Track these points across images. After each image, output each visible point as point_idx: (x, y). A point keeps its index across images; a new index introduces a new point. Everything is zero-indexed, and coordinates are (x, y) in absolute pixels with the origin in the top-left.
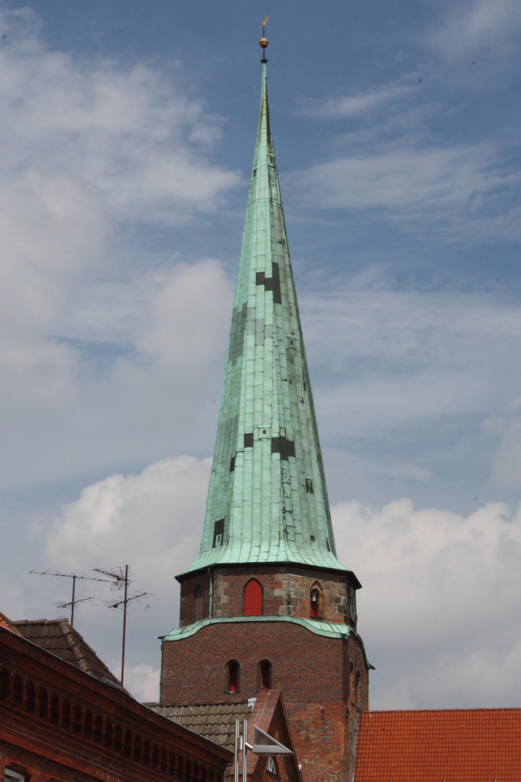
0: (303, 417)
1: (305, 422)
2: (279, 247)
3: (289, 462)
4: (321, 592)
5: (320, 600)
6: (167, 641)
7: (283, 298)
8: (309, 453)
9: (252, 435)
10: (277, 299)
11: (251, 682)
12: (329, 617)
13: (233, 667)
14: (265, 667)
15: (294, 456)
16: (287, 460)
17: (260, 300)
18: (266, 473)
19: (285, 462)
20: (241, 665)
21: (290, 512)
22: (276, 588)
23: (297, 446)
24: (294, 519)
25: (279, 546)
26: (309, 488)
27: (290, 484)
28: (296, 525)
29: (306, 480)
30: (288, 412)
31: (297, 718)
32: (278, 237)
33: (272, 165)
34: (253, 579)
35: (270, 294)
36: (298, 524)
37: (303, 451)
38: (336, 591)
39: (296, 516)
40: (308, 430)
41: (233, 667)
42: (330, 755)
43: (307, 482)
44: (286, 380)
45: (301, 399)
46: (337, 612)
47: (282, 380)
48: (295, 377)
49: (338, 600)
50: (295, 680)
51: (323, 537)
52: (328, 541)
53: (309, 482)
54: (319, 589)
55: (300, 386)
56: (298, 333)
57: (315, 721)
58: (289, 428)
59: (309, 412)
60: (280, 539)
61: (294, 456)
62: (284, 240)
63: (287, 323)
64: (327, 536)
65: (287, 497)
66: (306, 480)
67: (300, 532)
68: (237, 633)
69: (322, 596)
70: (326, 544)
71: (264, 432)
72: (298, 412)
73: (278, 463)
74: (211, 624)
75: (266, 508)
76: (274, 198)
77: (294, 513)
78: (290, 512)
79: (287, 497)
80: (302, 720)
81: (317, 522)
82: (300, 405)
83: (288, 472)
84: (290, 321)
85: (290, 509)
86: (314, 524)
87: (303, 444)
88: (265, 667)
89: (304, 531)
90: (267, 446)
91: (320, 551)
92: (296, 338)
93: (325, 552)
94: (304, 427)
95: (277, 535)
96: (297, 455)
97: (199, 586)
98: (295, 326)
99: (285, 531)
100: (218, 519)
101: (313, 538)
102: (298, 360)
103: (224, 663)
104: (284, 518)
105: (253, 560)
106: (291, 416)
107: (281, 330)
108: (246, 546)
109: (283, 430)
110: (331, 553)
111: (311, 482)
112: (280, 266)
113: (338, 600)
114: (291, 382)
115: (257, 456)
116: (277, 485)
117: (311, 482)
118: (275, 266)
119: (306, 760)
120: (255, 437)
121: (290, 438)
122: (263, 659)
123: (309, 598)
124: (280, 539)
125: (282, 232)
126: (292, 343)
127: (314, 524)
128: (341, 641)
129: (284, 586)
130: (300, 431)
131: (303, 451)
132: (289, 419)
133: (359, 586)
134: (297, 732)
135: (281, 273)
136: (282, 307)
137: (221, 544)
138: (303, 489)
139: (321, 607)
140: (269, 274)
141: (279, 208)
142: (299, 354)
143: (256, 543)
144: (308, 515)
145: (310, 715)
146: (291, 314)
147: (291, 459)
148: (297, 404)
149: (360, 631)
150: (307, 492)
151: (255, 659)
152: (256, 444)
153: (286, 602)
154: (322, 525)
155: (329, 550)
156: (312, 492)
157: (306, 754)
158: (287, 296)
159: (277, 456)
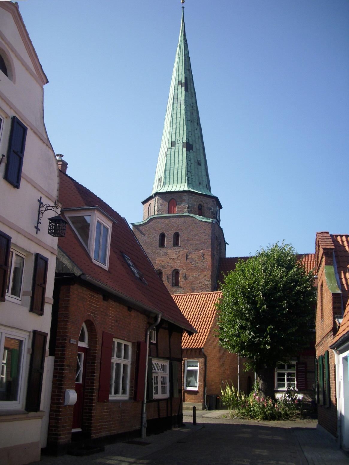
0: (197, 135)
1: (198, 138)
2: (188, 71)
3: (190, 152)
4: (203, 205)
5: (203, 208)
6: (134, 225)
7: (189, 90)
8: (199, 150)
9: (175, 142)
10: (186, 90)
11: (171, 242)
12: (207, 216)
13: (162, 236)
14: (177, 235)
15: (192, 150)
16: (189, 151)
17: (180, 90)
18: (180, 157)
19: (188, 152)
20: (166, 235)
21: (190, 172)
22: (183, 202)
23: (193, 146)
24: (192, 175)
25: (185, 185)
26: (199, 163)
27: (190, 161)
28: (193, 177)
29: (198, 160)
30: (190, 133)
31: (191, 257)
32: (187, 68)
33: (185, 43)
34: (173, 198)
35: (183, 88)
36: (194, 178)
37: (197, 149)
38: (210, 205)
39: (193, 174)
40: (199, 141)
41: (162, 236)
42: (205, 272)
43: (198, 161)
44: (189, 121)
45: (196, 129)
46: (210, 214)
47: (188, 121)
48: (193, 120)
49: (211, 209)
50: (190, 240)
51: (205, 183)
52: (207, 185)
53: (199, 161)
54: (202, 203)
55: (196, 124)
56: (195, 104)
57: (199, 258)
58: (190, 139)
59: (199, 134)
60: (185, 182)
61: (192, 150)
62: (190, 70)
63: (190, 99)
64: (207, 183)
65: (189, 166)
66: (198, 160)
67: (194, 180)
68: (165, 221)
69: (204, 206)
70: (206, 186)
71: (179, 141)
72: (195, 133)
73: (185, 153)
74: (153, 218)
75: (180, 171)
76: (186, 54)
77: (192, 173)
78: (190, 172)
79: (189, 166)
80: (193, 257)
81: (202, 177)
82: (196, 131)
83: (189, 156)
84: (192, 99)
85: (190, 171)
86: (201, 178)
87: (196, 146)
88: (176, 236)
89: (196, 180)
90: (181, 145)
91: (203, 189)
92: (194, 105)
93: (205, 189)
94: (197, 140)
95: (184, 181)
96: (194, 150)
97: (150, 204)
98: (194, 101)
99: (188, 179)
100: (160, 177)
101: (200, 184)
102: (195, 114)
103: (159, 234)
104: (187, 174)
105: (173, 190)
106: (191, 135)
107: (187, 102)
108: (171, 186)
109: (188, 140)
110: (208, 190)
111: (200, 161)
112: (188, 78)
113: (211, 209)
114: (191, 122)
115: (177, 150)
116: (185, 161)
117: (200, 161)
118: (186, 78)
119: (194, 275)
120: (176, 143)
121: (191, 143)
122: (176, 232)
123: (198, 207)
124: (185, 182)
125: (189, 67)
126: (192, 107)
127: (201, 178)
128: (210, 224)
129: (186, 201)
130: (195, 141)
131: (197, 149)
132: (190, 136)
133: (221, 207)
134: (191, 262)
135: (188, 81)
136: (189, 93)
137: (160, 187)
138: (196, 164)
139: (203, 211)
140: (183, 81)
141: (188, 58)
142: (196, 112)
143: (175, 184)
144: (198, 174)
145: (197, 255)
146: (192, 97)
147: (191, 151)
148: (194, 130)
149: (222, 225)
150: (198, 165)
151: (172, 233)
152: (177, 145)
153: (187, 208)
154: (204, 178)
155: (207, 189)
156: (200, 165)
157: (194, 272)
158: (191, 90)
159: (185, 149)
